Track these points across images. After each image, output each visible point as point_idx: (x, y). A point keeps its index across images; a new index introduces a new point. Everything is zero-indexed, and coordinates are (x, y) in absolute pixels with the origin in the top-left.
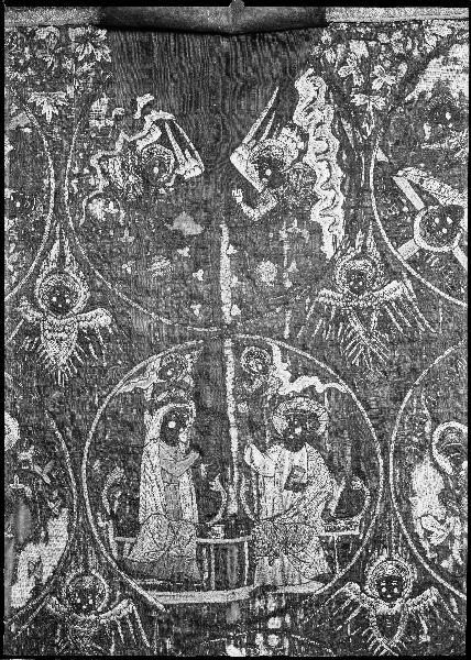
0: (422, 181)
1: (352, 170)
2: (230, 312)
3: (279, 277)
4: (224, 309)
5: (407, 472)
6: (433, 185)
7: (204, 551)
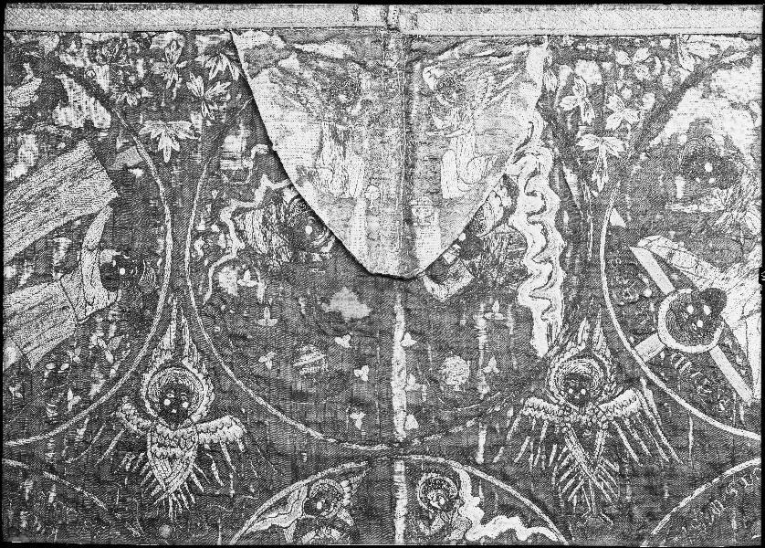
0: (671, 255)
1: (575, 237)
2: (404, 424)
3: (472, 378)
6: (684, 260)
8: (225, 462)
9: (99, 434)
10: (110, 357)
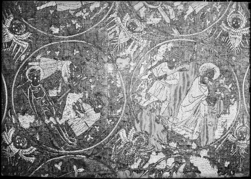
10: (218, 11)
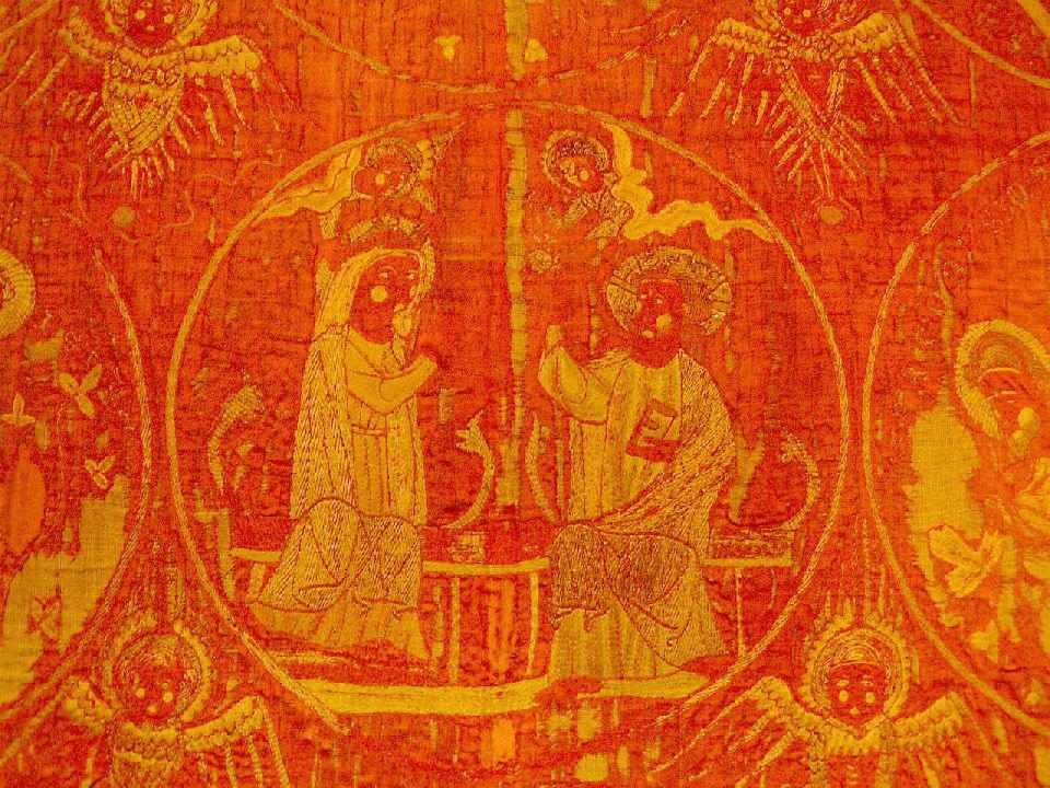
4: (512, 48)
5: (899, 422)
7: (437, 592)
8: (227, 107)
9: (28, 63)
